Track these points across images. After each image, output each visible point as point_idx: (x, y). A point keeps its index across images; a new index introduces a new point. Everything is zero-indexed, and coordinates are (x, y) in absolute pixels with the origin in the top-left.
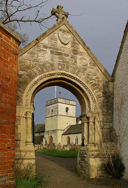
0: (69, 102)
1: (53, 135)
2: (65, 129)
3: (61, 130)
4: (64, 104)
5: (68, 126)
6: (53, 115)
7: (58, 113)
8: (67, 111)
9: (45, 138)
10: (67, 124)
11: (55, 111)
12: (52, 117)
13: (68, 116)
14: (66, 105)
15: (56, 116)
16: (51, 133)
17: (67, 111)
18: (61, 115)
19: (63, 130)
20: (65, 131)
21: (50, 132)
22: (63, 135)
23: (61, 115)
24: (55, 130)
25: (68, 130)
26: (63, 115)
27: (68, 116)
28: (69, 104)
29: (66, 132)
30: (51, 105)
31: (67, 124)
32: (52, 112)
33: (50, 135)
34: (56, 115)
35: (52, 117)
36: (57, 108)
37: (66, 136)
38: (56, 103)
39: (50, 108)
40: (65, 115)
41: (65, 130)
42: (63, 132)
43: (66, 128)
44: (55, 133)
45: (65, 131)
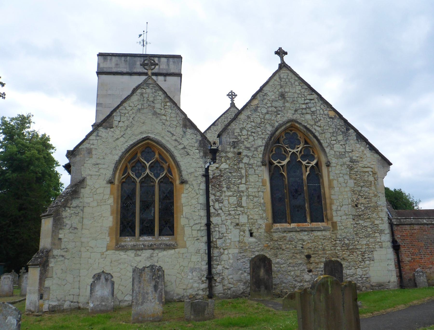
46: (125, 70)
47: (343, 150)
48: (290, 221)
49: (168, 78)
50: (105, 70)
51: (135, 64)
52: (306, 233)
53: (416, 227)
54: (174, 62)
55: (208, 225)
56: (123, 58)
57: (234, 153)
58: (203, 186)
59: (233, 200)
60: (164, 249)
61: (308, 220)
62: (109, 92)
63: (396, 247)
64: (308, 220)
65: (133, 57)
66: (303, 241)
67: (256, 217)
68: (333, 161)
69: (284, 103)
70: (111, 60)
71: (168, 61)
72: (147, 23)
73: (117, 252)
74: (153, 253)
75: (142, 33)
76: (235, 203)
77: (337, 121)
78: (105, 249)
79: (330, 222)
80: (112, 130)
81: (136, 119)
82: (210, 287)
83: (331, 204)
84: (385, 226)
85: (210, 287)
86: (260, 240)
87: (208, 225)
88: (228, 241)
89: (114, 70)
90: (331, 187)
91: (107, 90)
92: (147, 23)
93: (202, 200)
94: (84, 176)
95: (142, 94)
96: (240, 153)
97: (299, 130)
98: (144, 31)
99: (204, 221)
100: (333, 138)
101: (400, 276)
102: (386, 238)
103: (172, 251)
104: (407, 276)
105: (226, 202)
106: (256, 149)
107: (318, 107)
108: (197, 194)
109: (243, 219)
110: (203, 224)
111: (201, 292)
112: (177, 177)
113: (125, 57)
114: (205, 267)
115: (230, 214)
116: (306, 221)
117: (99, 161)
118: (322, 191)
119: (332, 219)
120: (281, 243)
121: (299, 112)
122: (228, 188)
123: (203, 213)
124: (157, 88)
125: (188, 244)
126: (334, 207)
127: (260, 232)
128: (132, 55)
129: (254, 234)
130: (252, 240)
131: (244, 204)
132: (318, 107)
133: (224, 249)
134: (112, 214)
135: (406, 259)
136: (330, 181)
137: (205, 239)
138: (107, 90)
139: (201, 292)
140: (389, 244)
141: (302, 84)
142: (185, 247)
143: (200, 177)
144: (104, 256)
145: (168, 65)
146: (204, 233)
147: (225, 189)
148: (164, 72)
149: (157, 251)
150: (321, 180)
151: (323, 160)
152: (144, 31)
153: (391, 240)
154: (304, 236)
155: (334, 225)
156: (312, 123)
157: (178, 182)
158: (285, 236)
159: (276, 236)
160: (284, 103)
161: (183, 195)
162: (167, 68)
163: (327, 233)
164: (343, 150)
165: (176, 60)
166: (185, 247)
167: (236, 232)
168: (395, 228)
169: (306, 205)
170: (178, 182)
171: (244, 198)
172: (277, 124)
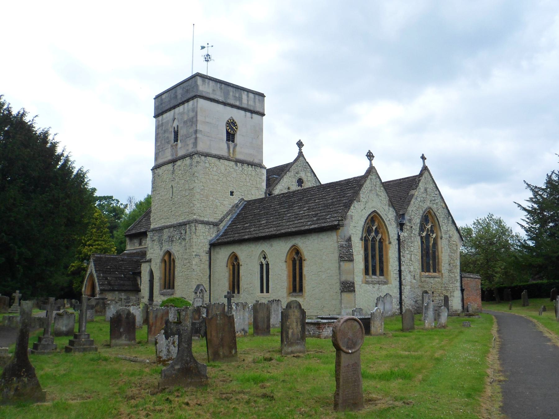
0: (240, 99)
1: (176, 249)
2: (221, 221)
3: (207, 223)
4: (221, 107)
5: (237, 206)
6: (181, 153)
7: (195, 144)
8: (231, 137)
9: (150, 261)
10: (232, 193)
11: (187, 136)
12: (173, 161)
13: (237, 161)
14: (228, 108)
15: (188, 161)
16: (171, 240)
17: (231, 137)
18: (207, 155)
19: (216, 225)
20: (223, 227)
21: (166, 234)
22: (214, 245)
23: (207, 155)
24: (184, 224)
25: (234, 222)
26: (214, 152)
27: (237, 161)
28: (237, 104)
29: (226, 233)
30: (172, 112)
31: (232, 193)
32: (176, 140)
33: (166, 247)
34: (191, 156)
35: (173, 161)
36: (193, 121)
37: (223, 255)
38: (188, 101)
39: (167, 122)
40: (223, 152)
41: (224, 223)
42: (210, 235)
43: (228, 214)
44: (184, 239)
45: (221, 226)
46: (221, 99)
47: (446, 230)
48: (426, 271)
49: (255, 116)
50: (204, 94)
51: (229, 94)
52: (432, 279)
53: (469, 279)
54: (259, 100)
55: (400, 271)
56: (219, 85)
57: (409, 226)
58: (397, 247)
59: (409, 256)
60: (384, 284)
61: (432, 271)
62: (208, 120)
63: (462, 290)
64: (432, 271)
65: (227, 86)
66: (432, 283)
67: (416, 268)
68: (443, 236)
69: (426, 195)
70: (208, 83)
71: (255, 98)
72: (194, 25)
73: (366, 285)
74: (379, 287)
75: (206, 45)
76: (409, 258)
77: (446, 210)
78: (361, 283)
79: (440, 273)
80: (359, 203)
81: (370, 197)
82: (401, 308)
83: (442, 262)
84: (458, 278)
85: (401, 308)
86: (417, 282)
87: (400, 271)
88: (407, 281)
89: (212, 96)
90: (442, 252)
91: (205, 117)
92: (194, 25)
93: (397, 255)
94: (350, 234)
95: (371, 179)
96: (412, 227)
97: (431, 215)
98: (208, 44)
99: (398, 269)
100: (444, 221)
101: (463, 307)
102: (458, 284)
103: (386, 286)
104: (465, 307)
105: (406, 258)
106: (417, 224)
107: (439, 200)
108: (395, 251)
109: (412, 269)
110: (397, 270)
111: (397, 311)
112: (387, 239)
113: (221, 84)
114: (399, 296)
115: (407, 265)
116: (430, 272)
117: (356, 225)
118: (437, 253)
119: (441, 271)
120: (424, 284)
121: (432, 202)
122: (407, 249)
123: (397, 263)
124: (377, 176)
125: (392, 281)
126: (443, 264)
127: (417, 277)
128: (226, 83)
129: (416, 278)
130: (415, 281)
131: (413, 260)
132: (439, 200)
133: (405, 286)
134: (363, 260)
135: (465, 297)
136: (442, 248)
137: (398, 279)
138: (205, 117)
139: (397, 311)
140: (459, 288)
141: (433, 183)
142: (391, 284)
143: (396, 240)
144: (361, 287)
145: (255, 102)
146: (398, 276)
147: (406, 249)
148: (252, 108)
149: (380, 285)
150: (436, 247)
151: (439, 235)
152: (208, 44)
153: (460, 286)
154: (432, 280)
155: (442, 274)
156: (436, 210)
157: (387, 242)
158: (426, 280)
159: (423, 279)
160: (426, 195)
161: (390, 251)
162: (254, 105)
163: (439, 280)
164: (446, 230)
165: (261, 97)
166: (391, 284)
167: (409, 276)
168: (462, 279)
169: (431, 262)
170: (387, 242)
171: (413, 256)
172: (424, 209)
